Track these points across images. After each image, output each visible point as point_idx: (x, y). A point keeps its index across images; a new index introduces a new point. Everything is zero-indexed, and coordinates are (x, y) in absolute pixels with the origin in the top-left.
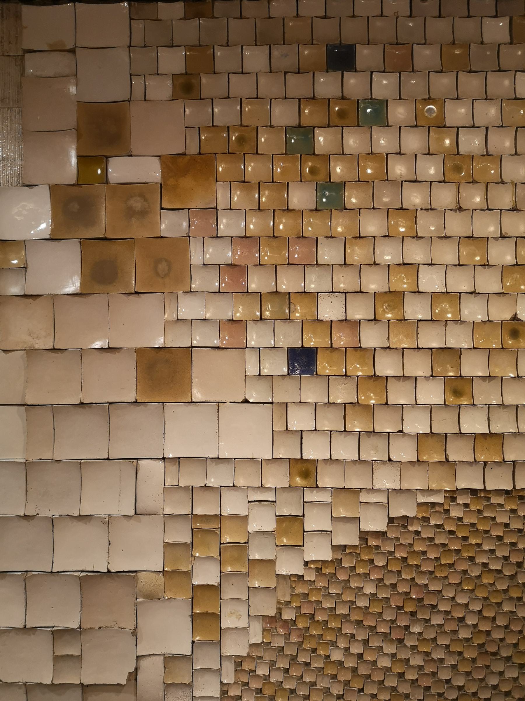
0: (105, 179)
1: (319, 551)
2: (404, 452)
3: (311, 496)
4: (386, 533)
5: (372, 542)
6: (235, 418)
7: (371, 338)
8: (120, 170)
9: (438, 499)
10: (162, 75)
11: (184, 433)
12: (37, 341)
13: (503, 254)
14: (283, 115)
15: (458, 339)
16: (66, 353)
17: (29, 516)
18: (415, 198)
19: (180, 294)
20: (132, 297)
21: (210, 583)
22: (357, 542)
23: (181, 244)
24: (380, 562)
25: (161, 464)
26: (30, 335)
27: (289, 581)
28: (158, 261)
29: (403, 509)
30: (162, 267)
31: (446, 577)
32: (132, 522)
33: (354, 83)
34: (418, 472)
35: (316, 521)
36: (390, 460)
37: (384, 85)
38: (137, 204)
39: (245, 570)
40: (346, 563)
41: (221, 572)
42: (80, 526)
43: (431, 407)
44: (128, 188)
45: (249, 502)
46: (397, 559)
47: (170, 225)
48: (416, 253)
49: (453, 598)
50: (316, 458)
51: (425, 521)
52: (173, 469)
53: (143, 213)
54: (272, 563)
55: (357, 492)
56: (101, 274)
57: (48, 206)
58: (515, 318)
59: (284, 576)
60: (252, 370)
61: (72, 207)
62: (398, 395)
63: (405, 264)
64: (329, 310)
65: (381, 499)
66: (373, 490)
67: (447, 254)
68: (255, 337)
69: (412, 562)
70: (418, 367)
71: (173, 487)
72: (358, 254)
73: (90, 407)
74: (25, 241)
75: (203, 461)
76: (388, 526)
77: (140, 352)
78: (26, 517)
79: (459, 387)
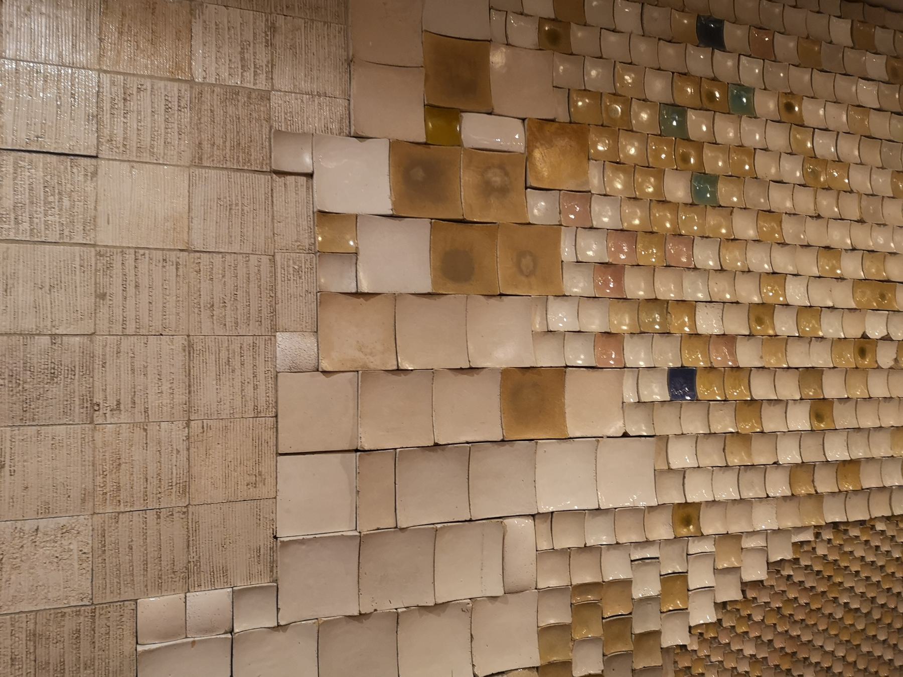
0: (456, 140)
1: (703, 614)
2: (779, 487)
3: (695, 547)
4: (762, 582)
5: (751, 594)
6: (616, 457)
7: (747, 356)
8: (476, 130)
9: (808, 536)
10: (527, 15)
11: (561, 481)
12: (372, 359)
13: (851, 267)
14: (657, 87)
15: (819, 358)
16: (411, 375)
17: (365, 614)
18: (780, 200)
19: (551, 298)
20: (492, 301)
21: (592, 672)
22: (739, 597)
23: (551, 234)
24: (758, 618)
25: (529, 522)
26: (360, 350)
27: (672, 655)
28: (521, 254)
29: (782, 552)
30: (527, 261)
31: (815, 624)
32: (497, 604)
33: (725, 64)
34: (790, 507)
35: (700, 577)
36: (768, 496)
37: (751, 71)
38: (496, 179)
39: (629, 647)
40: (726, 624)
41: (604, 655)
42: (431, 620)
43: (799, 434)
44: (489, 158)
45: (632, 561)
46: (772, 610)
47: (539, 209)
48: (783, 262)
49: (822, 647)
50: (697, 500)
51: (795, 564)
52: (544, 527)
53: (503, 191)
54: (656, 634)
55: (738, 537)
56: (458, 269)
57: (385, 169)
58: (864, 336)
59: (668, 649)
60: (630, 397)
61: (420, 175)
62: (772, 422)
63: (774, 273)
64: (708, 323)
65: (756, 542)
66: (754, 533)
67: (809, 265)
68: (637, 355)
69: (787, 612)
70: (789, 389)
71: (546, 552)
72: (733, 258)
73: (443, 450)
74: (357, 216)
75: (580, 514)
76: (768, 573)
77: (506, 373)
78: (362, 616)
79: (820, 408)
